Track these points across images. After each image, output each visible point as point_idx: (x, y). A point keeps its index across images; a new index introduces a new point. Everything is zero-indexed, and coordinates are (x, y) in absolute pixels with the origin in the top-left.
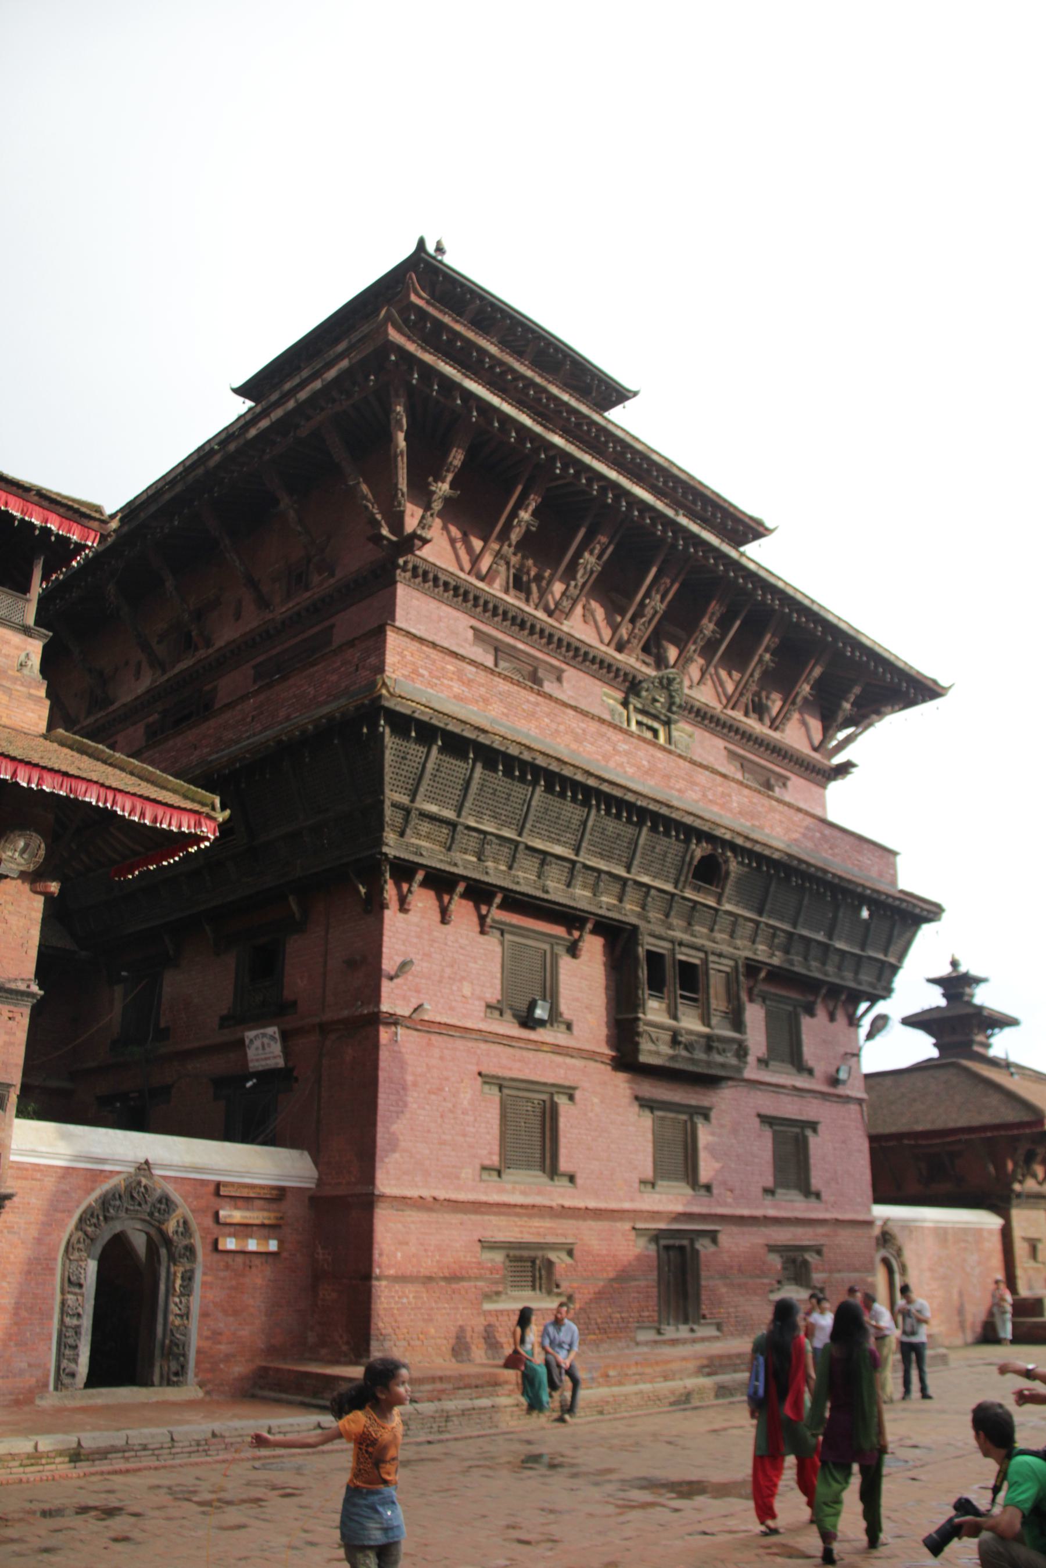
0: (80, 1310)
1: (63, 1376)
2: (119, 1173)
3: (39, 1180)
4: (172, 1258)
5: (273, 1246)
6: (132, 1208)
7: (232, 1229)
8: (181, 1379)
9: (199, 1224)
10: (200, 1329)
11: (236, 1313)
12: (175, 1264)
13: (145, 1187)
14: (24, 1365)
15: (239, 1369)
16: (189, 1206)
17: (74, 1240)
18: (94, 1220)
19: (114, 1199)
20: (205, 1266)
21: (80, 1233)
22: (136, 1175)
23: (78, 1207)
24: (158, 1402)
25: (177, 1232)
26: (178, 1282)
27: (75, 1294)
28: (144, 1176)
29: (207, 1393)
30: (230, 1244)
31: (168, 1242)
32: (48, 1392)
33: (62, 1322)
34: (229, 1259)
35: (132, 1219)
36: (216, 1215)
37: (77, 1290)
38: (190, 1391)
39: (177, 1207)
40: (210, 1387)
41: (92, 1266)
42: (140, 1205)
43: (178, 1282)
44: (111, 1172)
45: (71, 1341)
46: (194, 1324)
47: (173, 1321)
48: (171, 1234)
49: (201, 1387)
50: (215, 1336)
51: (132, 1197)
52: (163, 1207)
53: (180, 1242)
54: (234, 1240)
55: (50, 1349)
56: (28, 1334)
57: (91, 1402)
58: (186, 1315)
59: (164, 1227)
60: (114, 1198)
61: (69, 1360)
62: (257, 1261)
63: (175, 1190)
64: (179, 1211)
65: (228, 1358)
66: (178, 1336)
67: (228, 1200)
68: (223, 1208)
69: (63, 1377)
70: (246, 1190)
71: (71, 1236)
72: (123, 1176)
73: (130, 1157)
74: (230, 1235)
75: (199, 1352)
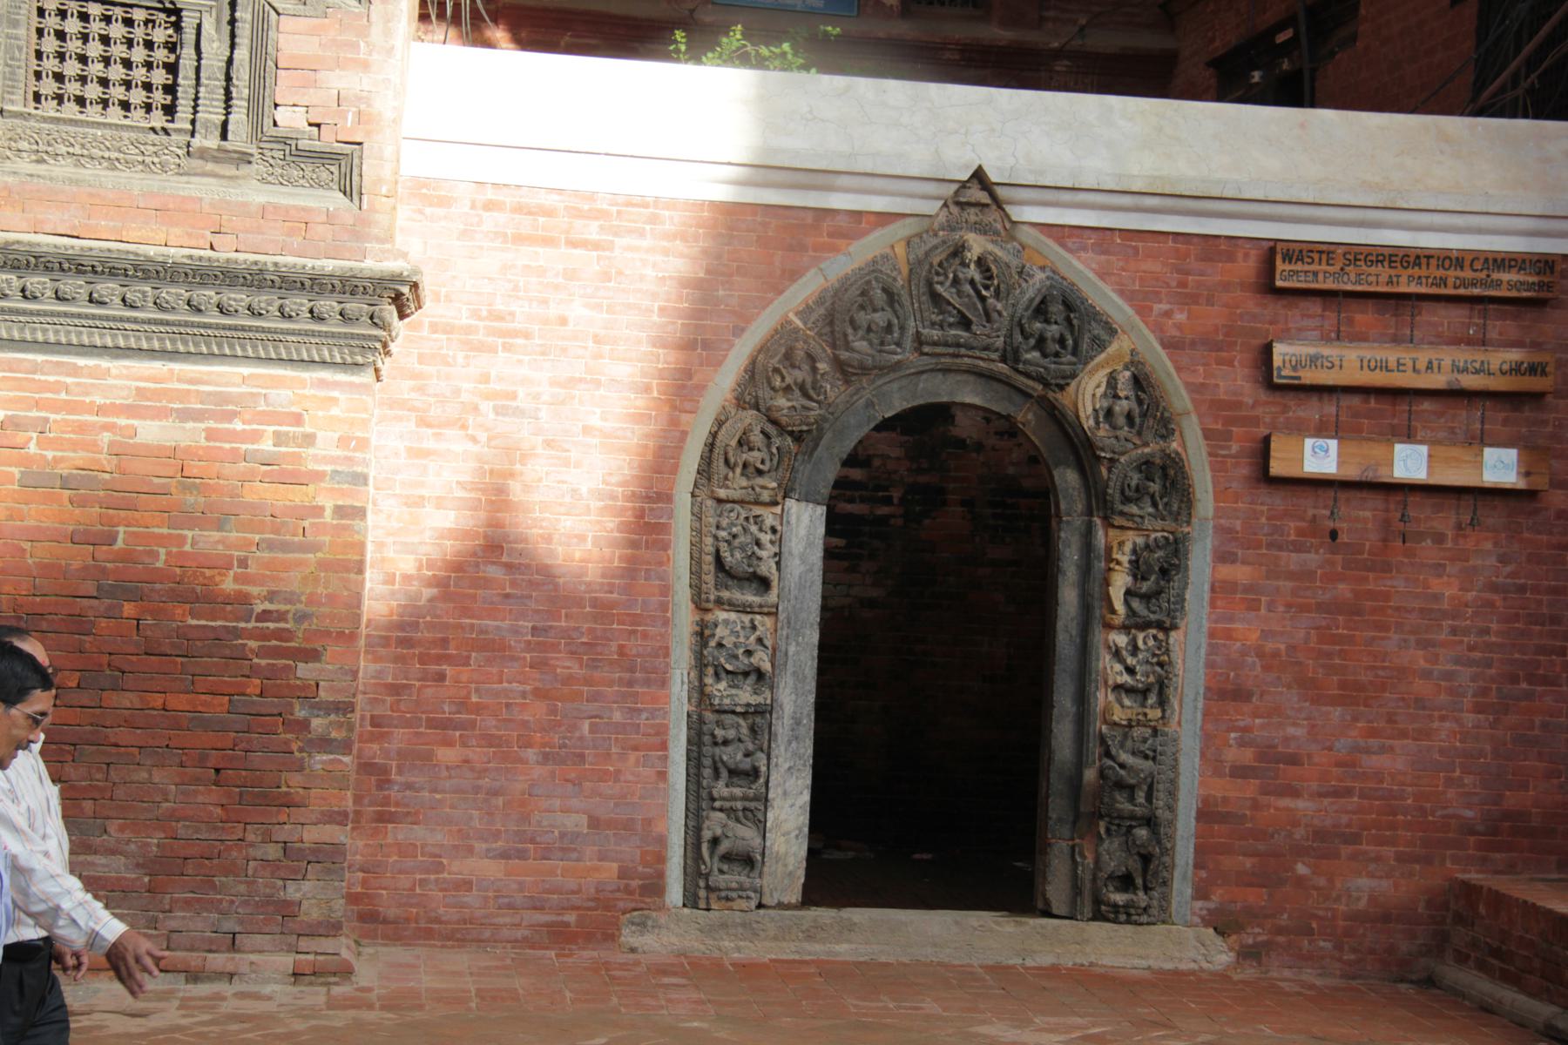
0: (762, 659)
1: (711, 863)
2: (885, 218)
3: (596, 246)
4: (1100, 503)
5: (1500, 467)
6: (935, 334)
7: (1330, 408)
8: (1141, 898)
9: (1193, 389)
10: (1207, 737)
11: (1352, 694)
12: (1109, 524)
13: (980, 262)
14: (576, 822)
15: (1365, 886)
16: (1157, 329)
17: (728, 438)
18: (799, 375)
19: (867, 304)
20: (1222, 531)
21: (749, 416)
22: (951, 227)
23: (739, 331)
24: (1054, 971)
25: (1109, 413)
26: (1120, 582)
27: (744, 609)
28: (982, 229)
29: (1248, 954)
30: (1321, 457)
31: (1082, 451)
32: (662, 908)
33: (700, 694)
34: (1314, 507)
35: (946, 371)
36: (1267, 350)
37: (751, 598)
38: (1182, 943)
39: (1113, 332)
40: (1254, 935)
41: (804, 525)
42: (965, 323)
43: (1120, 582)
44: (857, 215)
45: (733, 756)
46: (1187, 720)
47: (1107, 710)
48: (1088, 424)
49: (1220, 932)
50: (1273, 766)
51: (936, 298)
52: (1054, 330)
53: (1124, 451)
54: (1333, 444)
55: (662, 775)
56: (586, 726)
57: (817, 950)
58: (1158, 689)
59: (1064, 399)
60: (867, 304)
61: (730, 812)
62: (1444, 520)
63: (1102, 275)
64: (1119, 346)
65: (1324, 843)
66: (1124, 757)
67: (1315, 307)
68: (1286, 336)
69: (720, 867)
70: (1384, 272)
71: (720, 423)
72: (901, 230)
73: (918, 161)
74: (1321, 431)
75: (1206, 814)
